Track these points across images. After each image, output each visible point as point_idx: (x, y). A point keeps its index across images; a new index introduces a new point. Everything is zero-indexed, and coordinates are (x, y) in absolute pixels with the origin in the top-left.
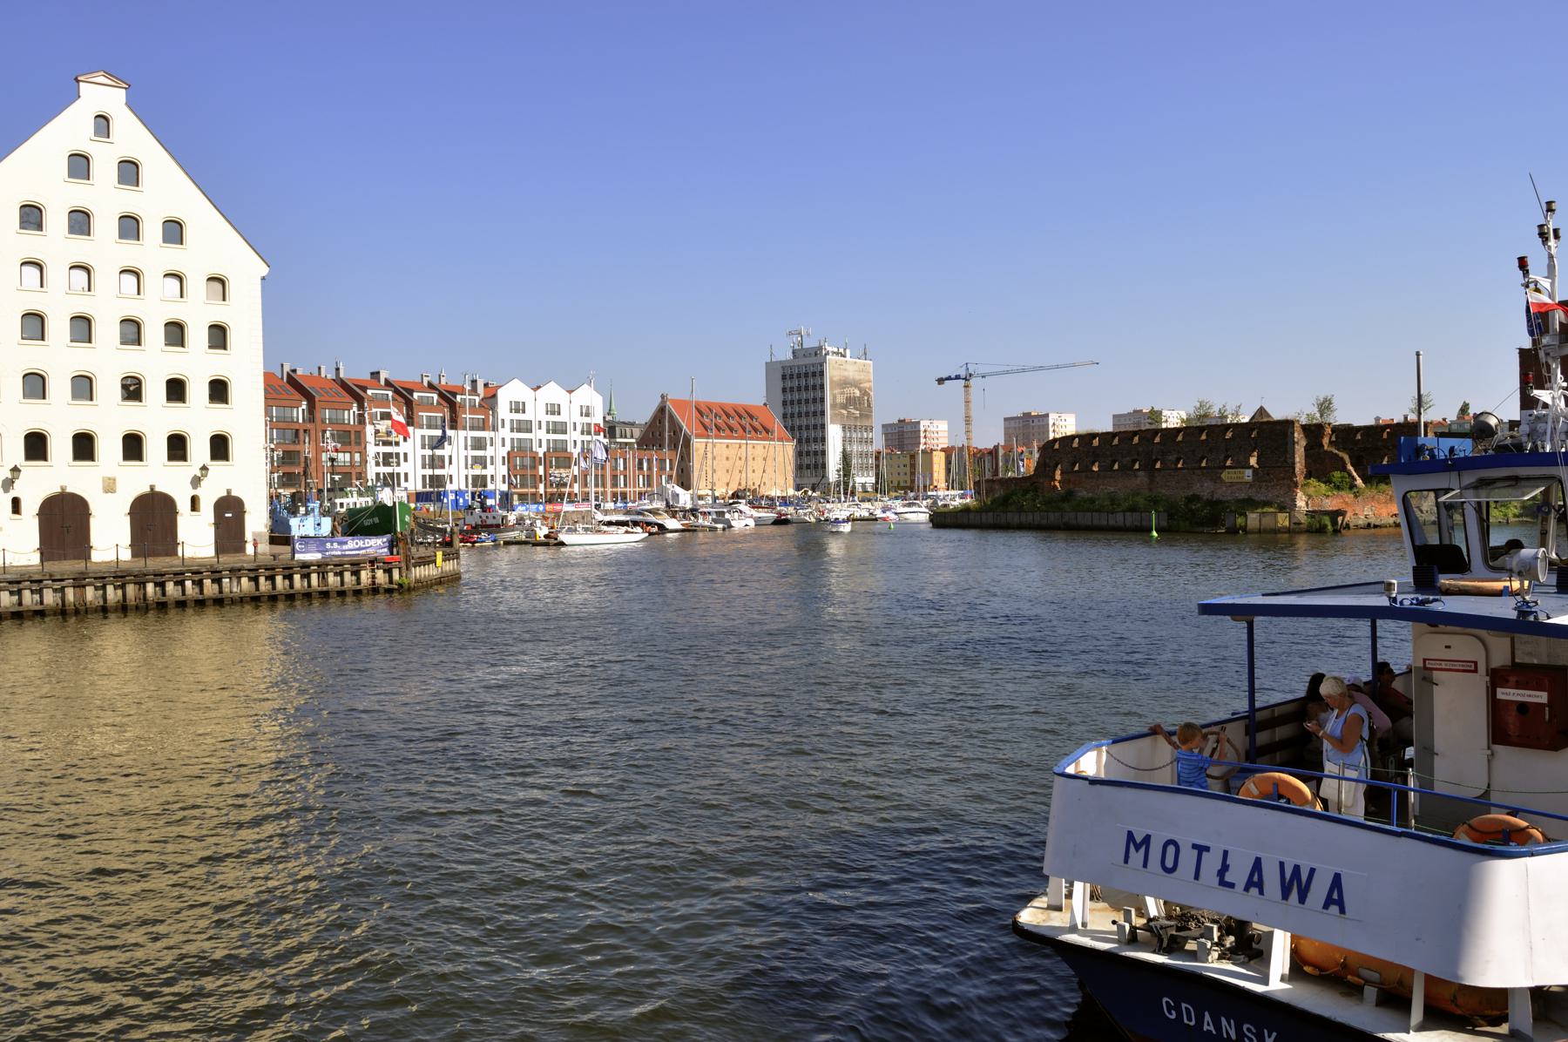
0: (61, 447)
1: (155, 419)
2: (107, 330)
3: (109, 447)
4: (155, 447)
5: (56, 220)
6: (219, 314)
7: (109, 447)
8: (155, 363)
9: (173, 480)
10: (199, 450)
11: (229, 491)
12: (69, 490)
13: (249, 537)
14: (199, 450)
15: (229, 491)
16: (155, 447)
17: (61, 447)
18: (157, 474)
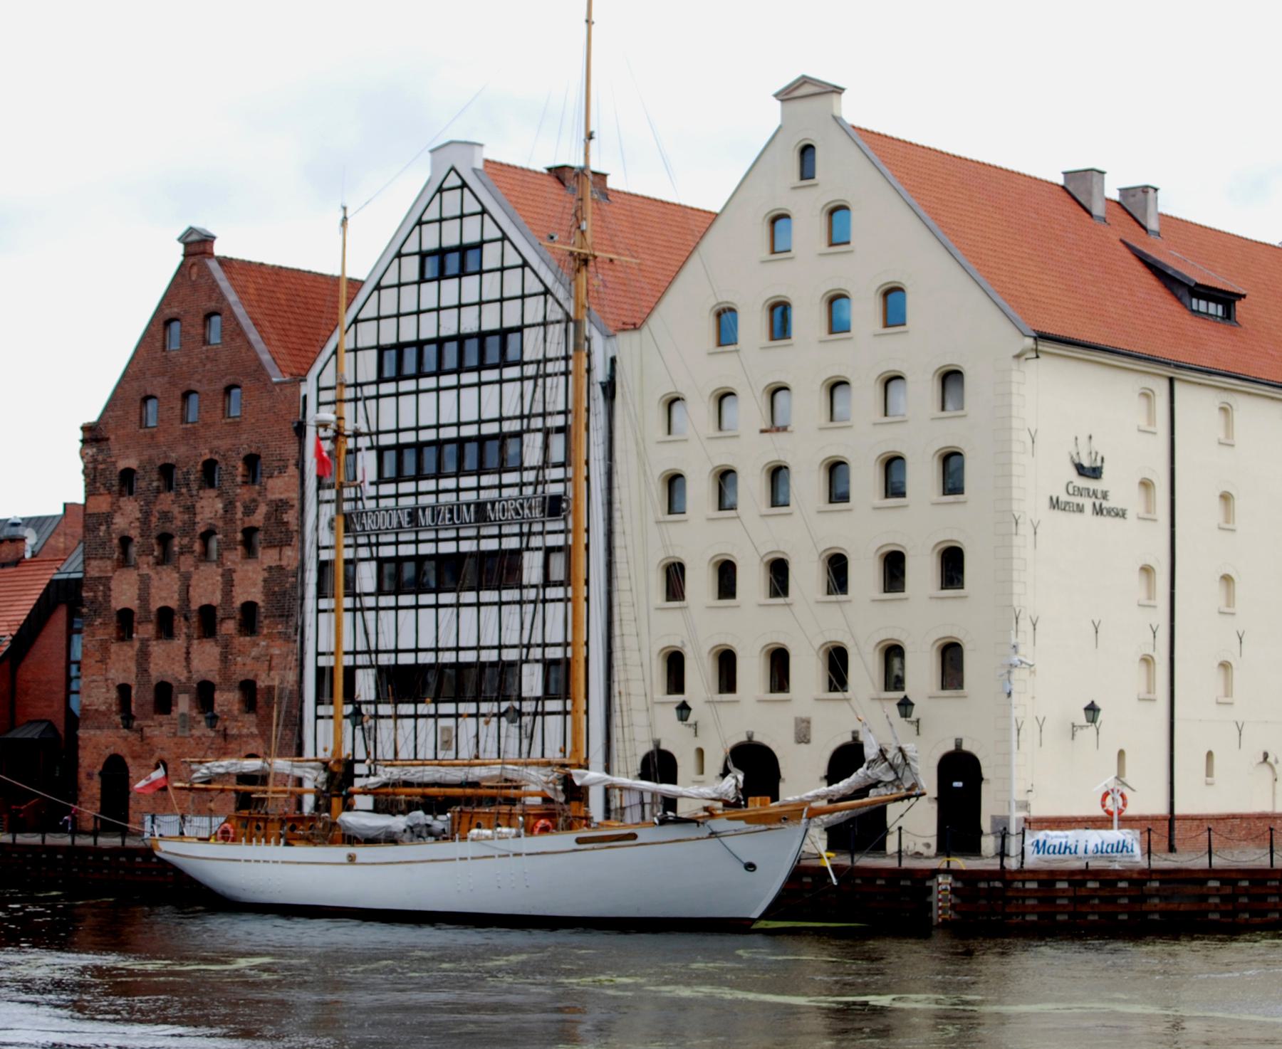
0: (752, 671)
1: (864, 619)
2: (807, 484)
3: (808, 670)
4: (865, 669)
5: (753, 324)
6: (950, 434)
7: (808, 670)
8: (864, 529)
9: (877, 726)
10: (921, 670)
11: (959, 743)
12: (757, 738)
13: (986, 824)
14: (921, 670)
15: (959, 743)
16: (865, 669)
17: (752, 671)
18: (865, 713)
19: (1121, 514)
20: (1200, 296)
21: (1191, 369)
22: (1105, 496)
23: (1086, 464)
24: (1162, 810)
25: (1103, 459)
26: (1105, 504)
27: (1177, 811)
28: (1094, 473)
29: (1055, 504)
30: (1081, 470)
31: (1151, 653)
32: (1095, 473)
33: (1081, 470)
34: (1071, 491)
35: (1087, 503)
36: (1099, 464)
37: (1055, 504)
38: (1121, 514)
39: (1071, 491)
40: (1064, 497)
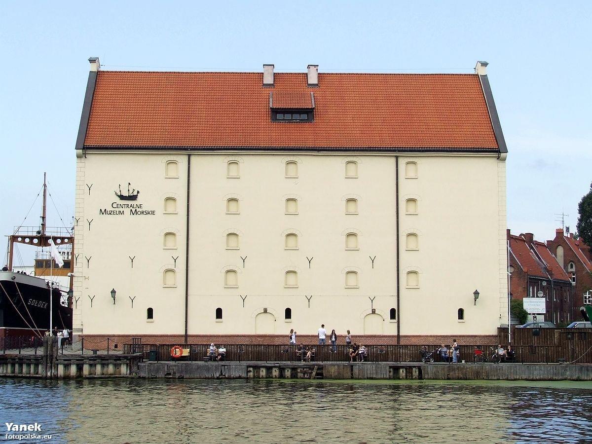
19: (153, 213)
20: (280, 113)
21: (204, 149)
22: (140, 206)
23: (126, 194)
24: (184, 333)
25: (138, 192)
26: (138, 210)
27: (189, 333)
28: (133, 198)
29: (103, 212)
30: (122, 197)
31: (173, 267)
32: (133, 198)
33: (122, 197)
34: (115, 205)
35: (127, 211)
36: (135, 193)
37: (103, 212)
38: (153, 213)
39: (115, 205)
40: (109, 209)
